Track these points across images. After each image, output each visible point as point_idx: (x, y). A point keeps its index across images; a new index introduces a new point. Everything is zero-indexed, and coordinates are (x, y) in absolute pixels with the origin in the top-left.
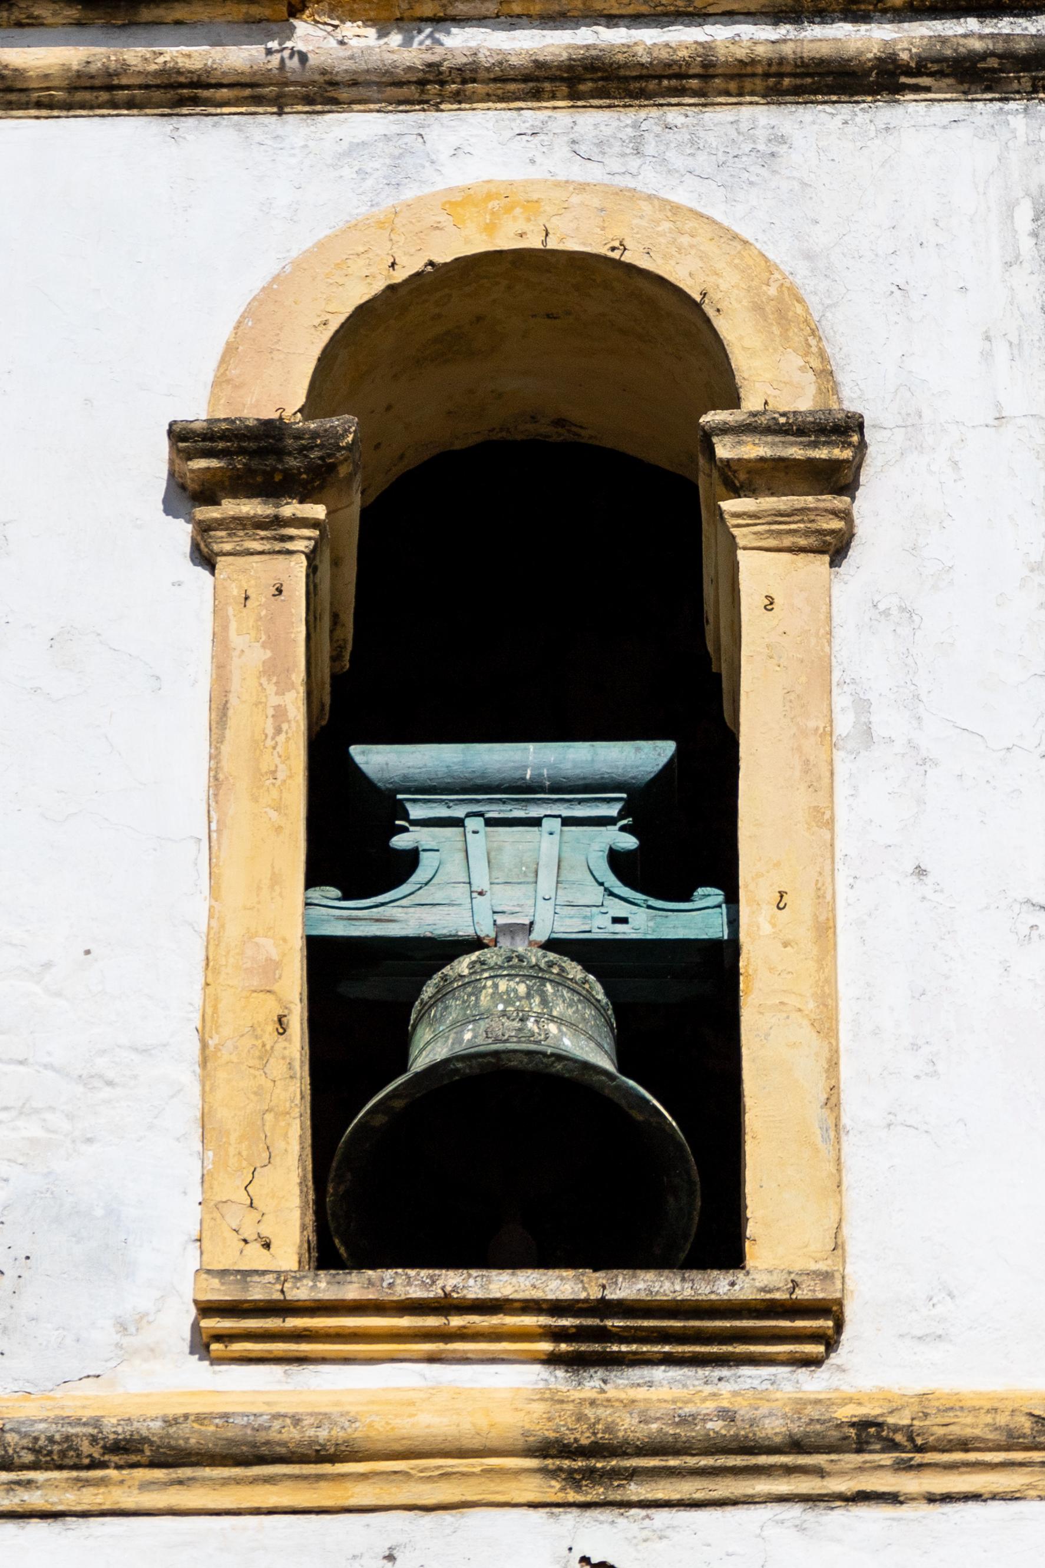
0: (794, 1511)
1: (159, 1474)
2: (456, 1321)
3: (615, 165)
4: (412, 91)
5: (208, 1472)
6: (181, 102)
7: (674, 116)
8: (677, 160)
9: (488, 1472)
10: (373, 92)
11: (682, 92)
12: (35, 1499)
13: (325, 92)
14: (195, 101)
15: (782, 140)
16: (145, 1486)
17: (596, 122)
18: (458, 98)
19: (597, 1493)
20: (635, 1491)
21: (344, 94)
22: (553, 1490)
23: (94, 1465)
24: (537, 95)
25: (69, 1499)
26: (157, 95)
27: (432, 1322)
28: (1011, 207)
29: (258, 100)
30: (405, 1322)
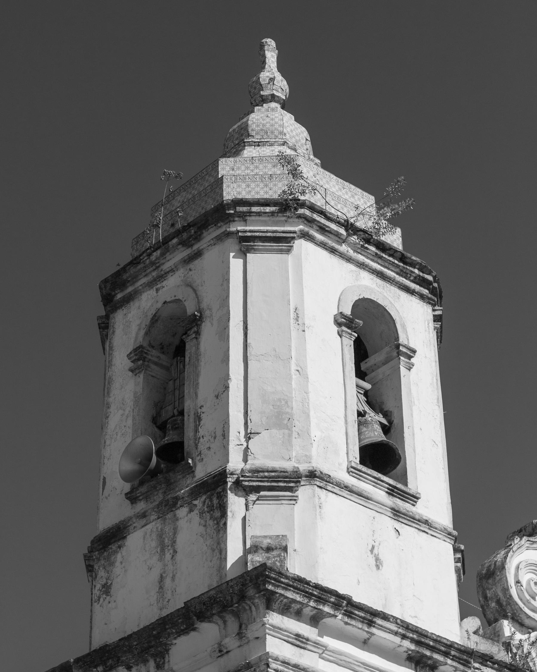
0: (417, 530)
1: (349, 493)
2: (379, 482)
3: (381, 290)
4: (359, 265)
5: (354, 495)
6: (332, 252)
7: (388, 285)
8: (388, 293)
9: (386, 509)
10: (355, 263)
11: (389, 282)
12: (335, 491)
13: (349, 260)
14: (333, 252)
15: (400, 296)
16: (347, 494)
17: (379, 281)
18: (364, 269)
19: (396, 518)
20: (400, 519)
21: (351, 261)
22: (391, 515)
23: (342, 488)
24: (373, 273)
25: (338, 492)
26: (330, 249)
27: (376, 481)
28: (425, 321)
29: (341, 256)
30: (373, 479)
